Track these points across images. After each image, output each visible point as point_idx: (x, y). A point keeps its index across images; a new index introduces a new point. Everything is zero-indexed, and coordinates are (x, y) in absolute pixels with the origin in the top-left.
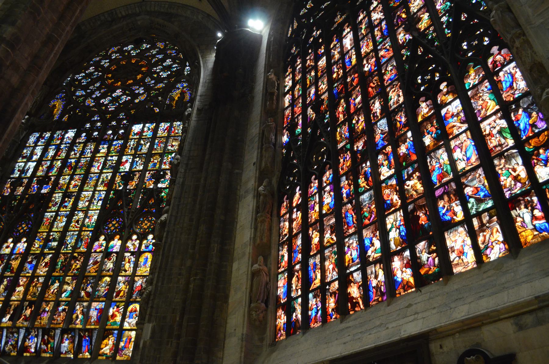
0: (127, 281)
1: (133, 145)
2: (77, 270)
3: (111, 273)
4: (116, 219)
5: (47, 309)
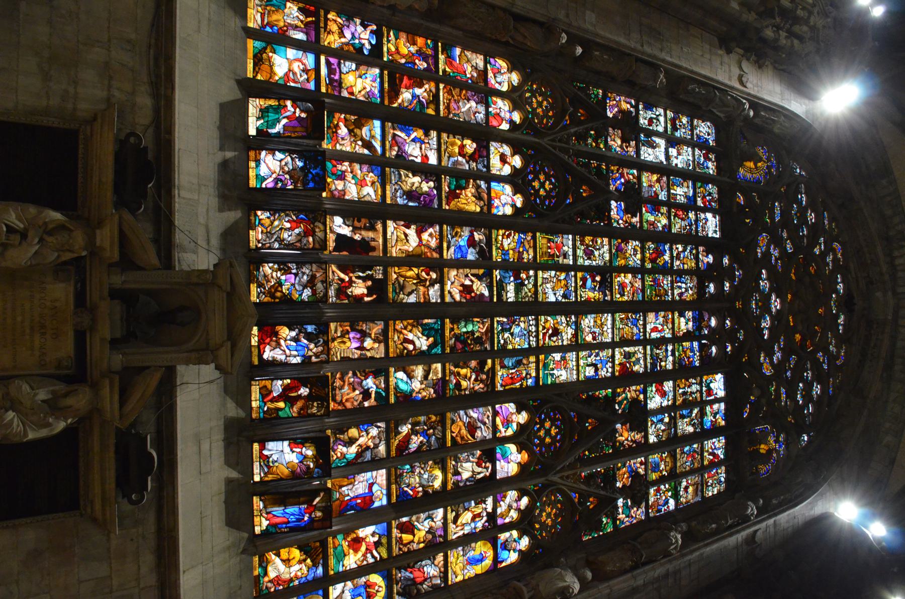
0: (434, 536)
2: (458, 385)
5: (368, 343)
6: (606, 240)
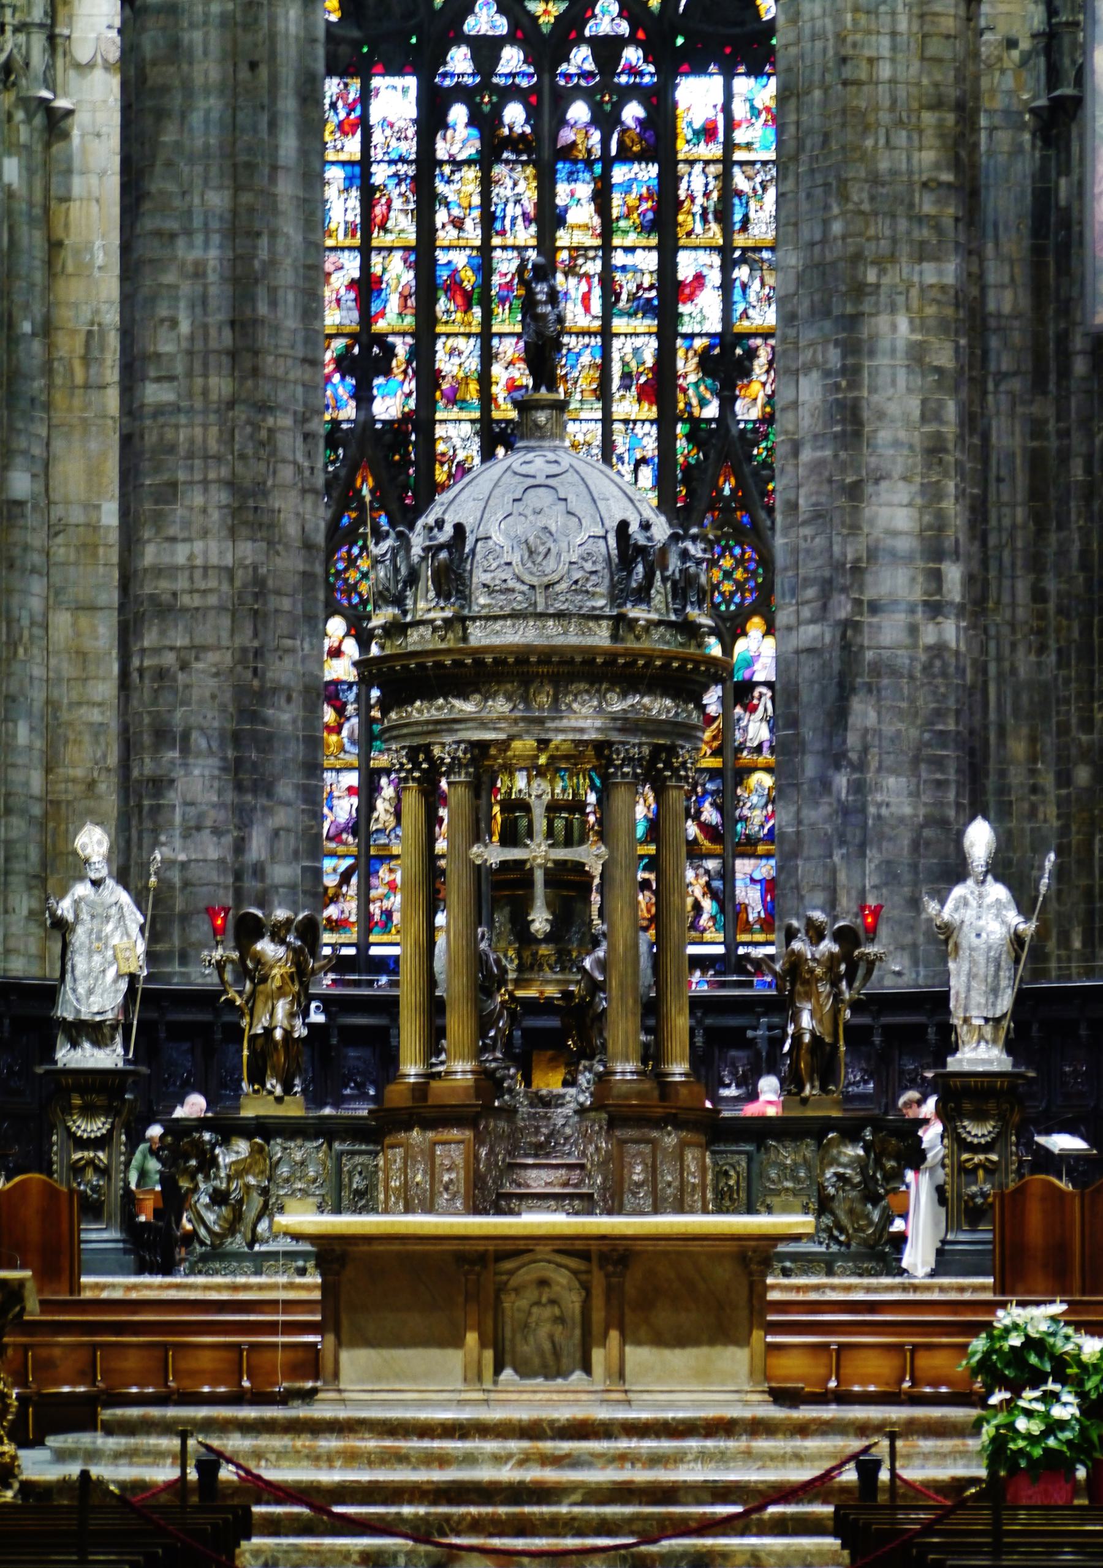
1: (707, 195)
3: (767, 757)
4: (731, 549)
6: (440, 431)
